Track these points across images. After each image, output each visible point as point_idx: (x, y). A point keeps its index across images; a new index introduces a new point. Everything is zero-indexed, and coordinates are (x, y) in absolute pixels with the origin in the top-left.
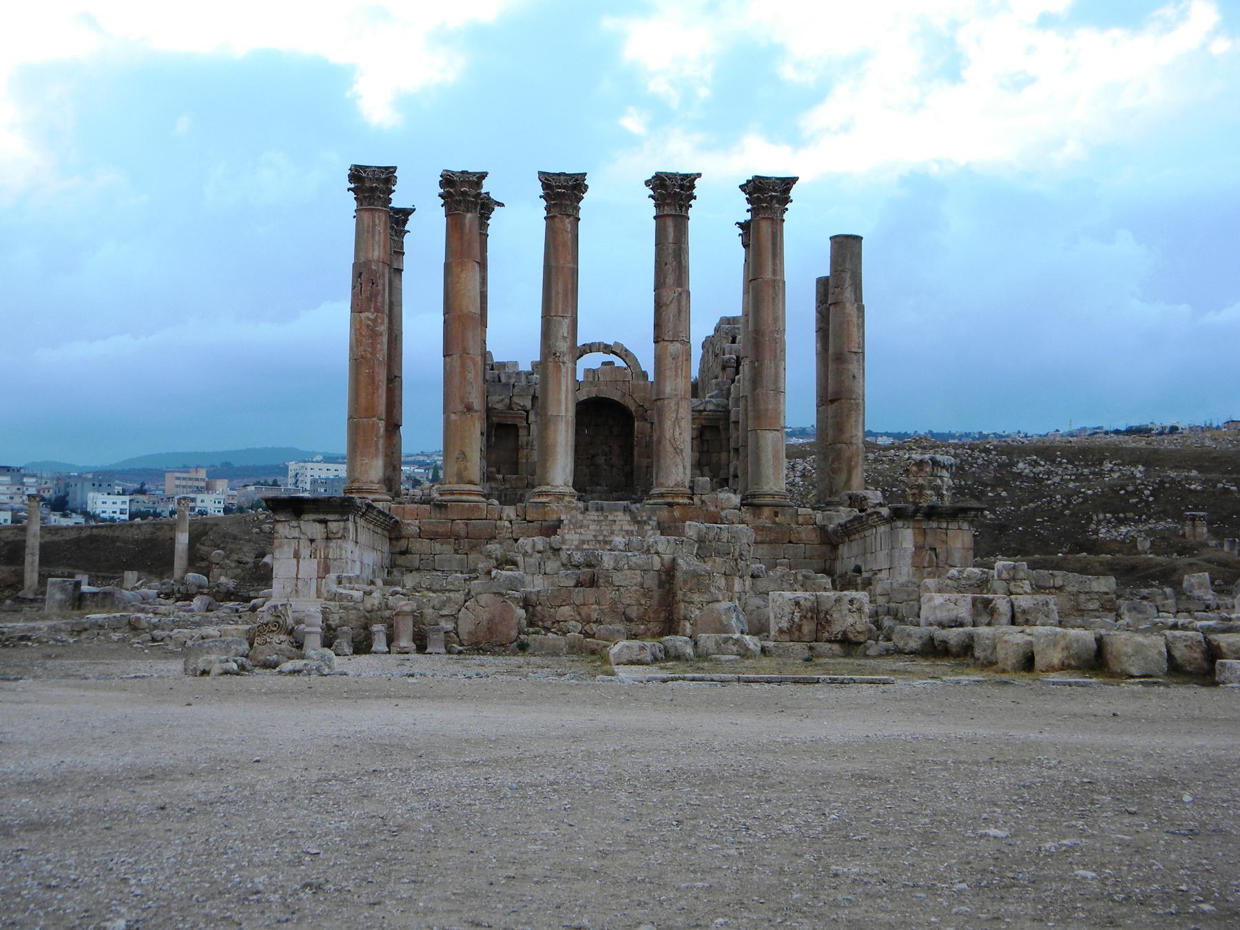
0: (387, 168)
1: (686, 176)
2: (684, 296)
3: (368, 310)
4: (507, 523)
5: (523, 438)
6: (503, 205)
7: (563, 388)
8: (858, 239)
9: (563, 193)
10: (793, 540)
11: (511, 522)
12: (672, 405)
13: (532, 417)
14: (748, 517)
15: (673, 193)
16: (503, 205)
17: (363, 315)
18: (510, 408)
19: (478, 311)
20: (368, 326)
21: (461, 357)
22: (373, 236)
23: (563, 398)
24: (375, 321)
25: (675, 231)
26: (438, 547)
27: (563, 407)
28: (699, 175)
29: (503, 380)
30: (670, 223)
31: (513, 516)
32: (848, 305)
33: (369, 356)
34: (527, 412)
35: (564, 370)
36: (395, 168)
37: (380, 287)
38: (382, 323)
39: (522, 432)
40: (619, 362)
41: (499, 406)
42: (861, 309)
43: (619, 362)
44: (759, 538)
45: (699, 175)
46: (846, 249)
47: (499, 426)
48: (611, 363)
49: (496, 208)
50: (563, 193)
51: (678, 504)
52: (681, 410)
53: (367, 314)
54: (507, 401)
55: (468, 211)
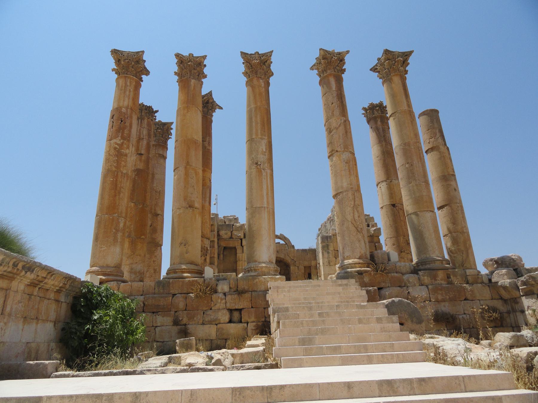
0: (138, 53)
1: (339, 54)
2: (347, 122)
3: (116, 137)
4: (221, 295)
5: (239, 255)
6: (222, 108)
7: (265, 187)
8: (437, 111)
9: (258, 68)
10: (469, 297)
11: (225, 294)
12: (350, 195)
13: (244, 242)
14: (426, 279)
15: (331, 66)
16: (222, 108)
17: (112, 142)
18: (231, 238)
19: (199, 137)
20: (115, 148)
21: (186, 168)
22: (125, 92)
23: (265, 194)
24: (121, 145)
25: (336, 83)
26: (160, 319)
27: (265, 201)
28: (348, 52)
29: (227, 223)
30: (332, 81)
31: (226, 288)
32: (441, 147)
33: (114, 169)
34: (241, 240)
35: (264, 174)
36: (143, 52)
37: (127, 124)
38: (128, 148)
39: (239, 251)
40: (282, 242)
41: (225, 236)
42: (448, 148)
43: (282, 242)
44: (440, 297)
45: (348, 52)
46: (432, 116)
47: (225, 248)
48: (279, 243)
49: (217, 110)
50: (258, 68)
51: (366, 272)
52: (356, 199)
53: (114, 141)
54: (229, 234)
55: (194, 78)
